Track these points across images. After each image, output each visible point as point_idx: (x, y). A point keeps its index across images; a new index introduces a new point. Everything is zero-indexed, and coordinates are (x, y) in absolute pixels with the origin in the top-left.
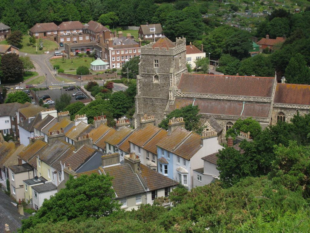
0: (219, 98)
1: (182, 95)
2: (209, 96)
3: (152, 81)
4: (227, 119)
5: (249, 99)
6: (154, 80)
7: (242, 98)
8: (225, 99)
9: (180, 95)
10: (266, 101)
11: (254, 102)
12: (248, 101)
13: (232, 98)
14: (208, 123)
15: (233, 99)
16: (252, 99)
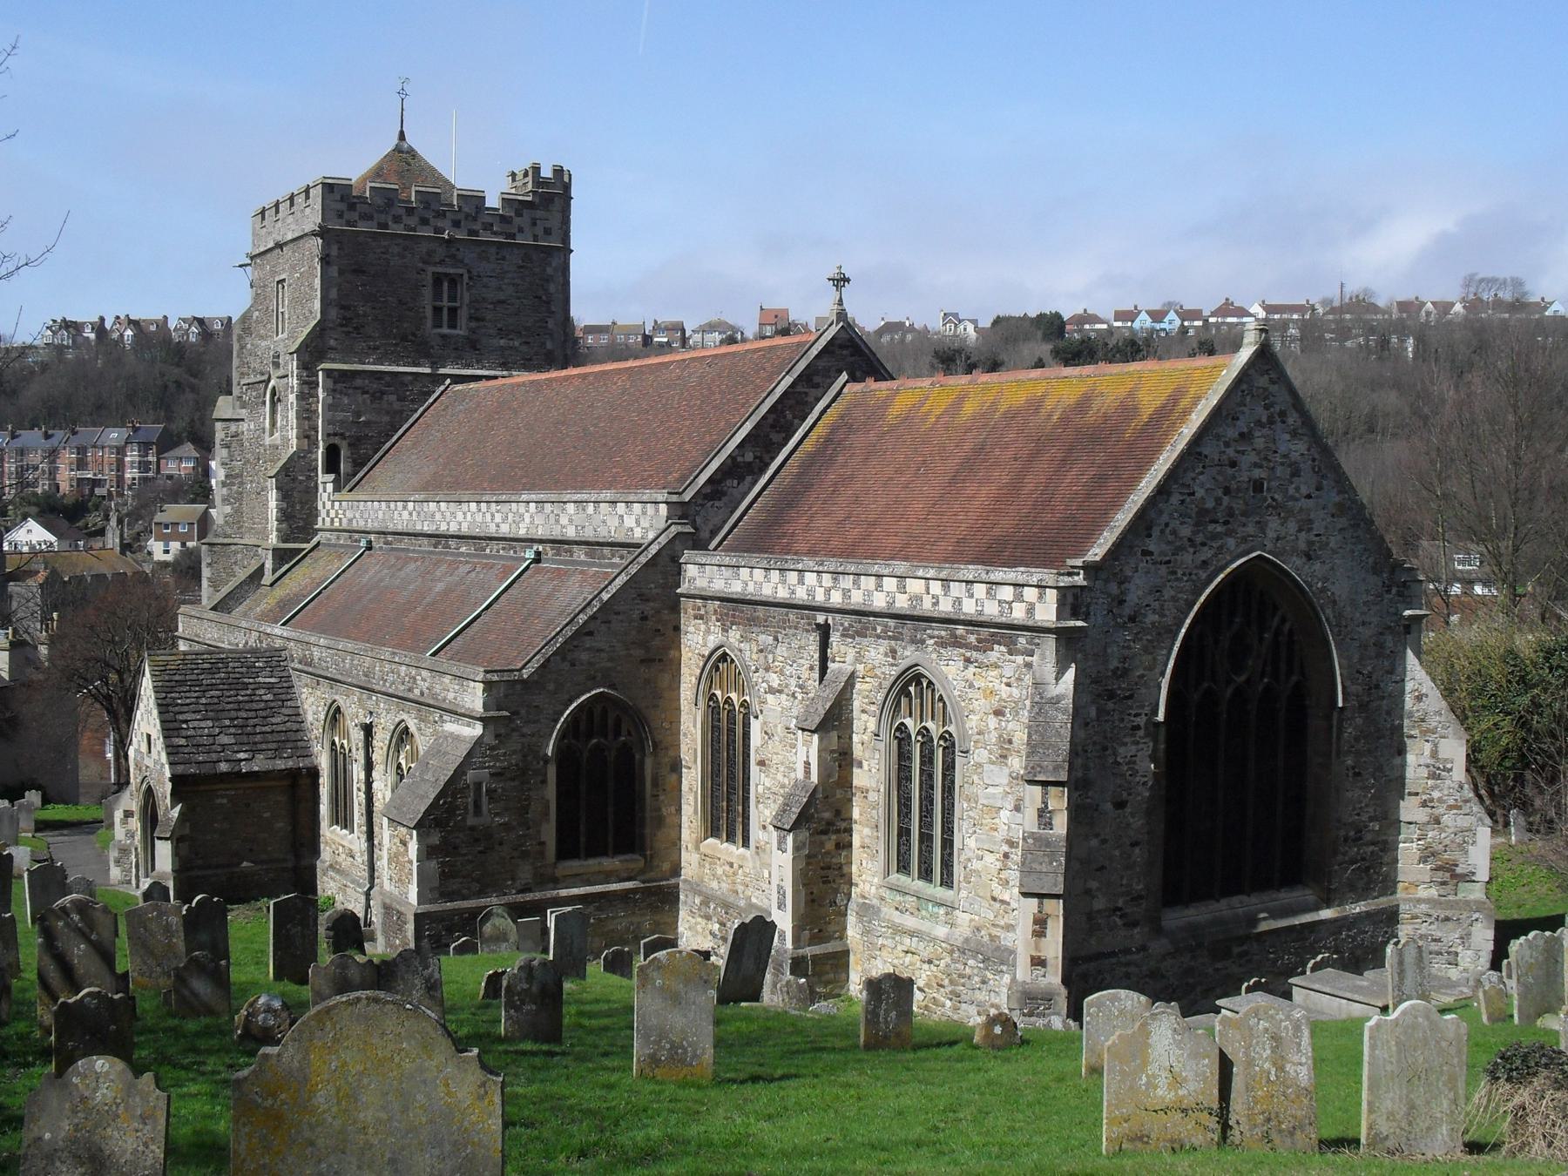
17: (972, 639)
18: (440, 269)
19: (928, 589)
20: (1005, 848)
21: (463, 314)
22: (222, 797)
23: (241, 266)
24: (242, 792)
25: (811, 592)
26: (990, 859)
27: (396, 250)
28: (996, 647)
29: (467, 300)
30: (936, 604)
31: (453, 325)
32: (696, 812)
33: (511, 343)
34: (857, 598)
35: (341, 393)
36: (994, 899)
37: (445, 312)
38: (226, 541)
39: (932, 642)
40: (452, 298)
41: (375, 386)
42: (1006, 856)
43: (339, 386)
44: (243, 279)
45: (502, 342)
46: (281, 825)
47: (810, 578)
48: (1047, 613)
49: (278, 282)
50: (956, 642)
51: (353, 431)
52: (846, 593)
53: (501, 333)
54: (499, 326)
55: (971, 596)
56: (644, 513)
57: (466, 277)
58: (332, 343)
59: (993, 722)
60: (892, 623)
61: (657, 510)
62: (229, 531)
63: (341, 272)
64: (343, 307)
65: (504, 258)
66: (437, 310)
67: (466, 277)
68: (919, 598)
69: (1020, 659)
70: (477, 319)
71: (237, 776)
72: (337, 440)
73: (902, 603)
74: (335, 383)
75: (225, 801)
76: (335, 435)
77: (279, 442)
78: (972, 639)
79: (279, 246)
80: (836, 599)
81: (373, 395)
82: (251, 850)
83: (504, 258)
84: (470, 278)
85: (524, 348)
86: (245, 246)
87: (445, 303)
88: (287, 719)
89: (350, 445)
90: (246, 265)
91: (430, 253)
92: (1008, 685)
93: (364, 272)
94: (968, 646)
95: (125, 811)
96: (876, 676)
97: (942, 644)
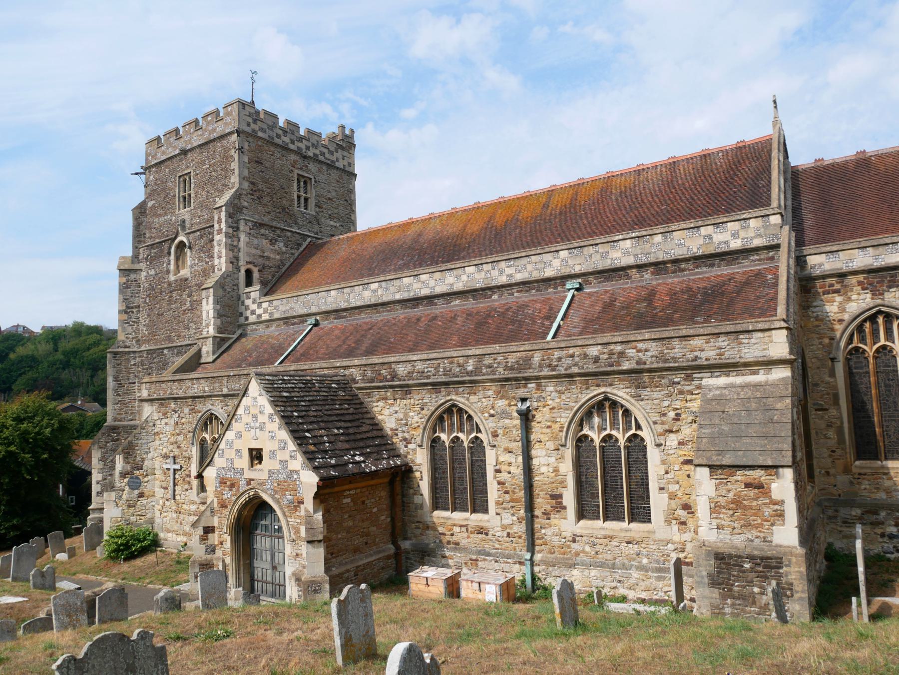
1: (266, 311)
2: (375, 291)
3: (168, 272)
4: (436, 386)
5: (605, 256)
6: (172, 267)
7: (556, 263)
8: (459, 286)
9: (258, 312)
10: (736, 244)
11: (640, 267)
12: (600, 267)
13: (495, 273)
15: (503, 280)
16: (626, 253)
18: (301, 173)
21: (312, 203)
22: (348, 496)
23: (136, 174)
24: (358, 491)
27: (279, 155)
29: (314, 195)
31: (306, 207)
32: (841, 441)
33: (335, 224)
35: (254, 236)
37: (302, 199)
38: (127, 350)
40: (306, 193)
41: (272, 235)
43: (252, 232)
44: (140, 181)
45: (332, 223)
46: (383, 518)
49: (180, 177)
51: (261, 261)
53: (331, 217)
54: (330, 213)
57: (313, 180)
58: (246, 204)
62: (128, 343)
63: (250, 161)
64: (252, 183)
65: (330, 174)
66: (299, 197)
67: (313, 180)
70: (320, 207)
71: (363, 475)
72: (250, 266)
74: (250, 229)
75: (349, 500)
76: (250, 263)
77: (189, 275)
79: (184, 152)
81: (271, 241)
82: (366, 543)
83: (330, 174)
84: (315, 182)
85: (341, 228)
86: (140, 162)
87: (302, 193)
88: (371, 428)
89: (259, 271)
90: (141, 173)
91: (295, 162)
93: (262, 164)
95: (205, 528)
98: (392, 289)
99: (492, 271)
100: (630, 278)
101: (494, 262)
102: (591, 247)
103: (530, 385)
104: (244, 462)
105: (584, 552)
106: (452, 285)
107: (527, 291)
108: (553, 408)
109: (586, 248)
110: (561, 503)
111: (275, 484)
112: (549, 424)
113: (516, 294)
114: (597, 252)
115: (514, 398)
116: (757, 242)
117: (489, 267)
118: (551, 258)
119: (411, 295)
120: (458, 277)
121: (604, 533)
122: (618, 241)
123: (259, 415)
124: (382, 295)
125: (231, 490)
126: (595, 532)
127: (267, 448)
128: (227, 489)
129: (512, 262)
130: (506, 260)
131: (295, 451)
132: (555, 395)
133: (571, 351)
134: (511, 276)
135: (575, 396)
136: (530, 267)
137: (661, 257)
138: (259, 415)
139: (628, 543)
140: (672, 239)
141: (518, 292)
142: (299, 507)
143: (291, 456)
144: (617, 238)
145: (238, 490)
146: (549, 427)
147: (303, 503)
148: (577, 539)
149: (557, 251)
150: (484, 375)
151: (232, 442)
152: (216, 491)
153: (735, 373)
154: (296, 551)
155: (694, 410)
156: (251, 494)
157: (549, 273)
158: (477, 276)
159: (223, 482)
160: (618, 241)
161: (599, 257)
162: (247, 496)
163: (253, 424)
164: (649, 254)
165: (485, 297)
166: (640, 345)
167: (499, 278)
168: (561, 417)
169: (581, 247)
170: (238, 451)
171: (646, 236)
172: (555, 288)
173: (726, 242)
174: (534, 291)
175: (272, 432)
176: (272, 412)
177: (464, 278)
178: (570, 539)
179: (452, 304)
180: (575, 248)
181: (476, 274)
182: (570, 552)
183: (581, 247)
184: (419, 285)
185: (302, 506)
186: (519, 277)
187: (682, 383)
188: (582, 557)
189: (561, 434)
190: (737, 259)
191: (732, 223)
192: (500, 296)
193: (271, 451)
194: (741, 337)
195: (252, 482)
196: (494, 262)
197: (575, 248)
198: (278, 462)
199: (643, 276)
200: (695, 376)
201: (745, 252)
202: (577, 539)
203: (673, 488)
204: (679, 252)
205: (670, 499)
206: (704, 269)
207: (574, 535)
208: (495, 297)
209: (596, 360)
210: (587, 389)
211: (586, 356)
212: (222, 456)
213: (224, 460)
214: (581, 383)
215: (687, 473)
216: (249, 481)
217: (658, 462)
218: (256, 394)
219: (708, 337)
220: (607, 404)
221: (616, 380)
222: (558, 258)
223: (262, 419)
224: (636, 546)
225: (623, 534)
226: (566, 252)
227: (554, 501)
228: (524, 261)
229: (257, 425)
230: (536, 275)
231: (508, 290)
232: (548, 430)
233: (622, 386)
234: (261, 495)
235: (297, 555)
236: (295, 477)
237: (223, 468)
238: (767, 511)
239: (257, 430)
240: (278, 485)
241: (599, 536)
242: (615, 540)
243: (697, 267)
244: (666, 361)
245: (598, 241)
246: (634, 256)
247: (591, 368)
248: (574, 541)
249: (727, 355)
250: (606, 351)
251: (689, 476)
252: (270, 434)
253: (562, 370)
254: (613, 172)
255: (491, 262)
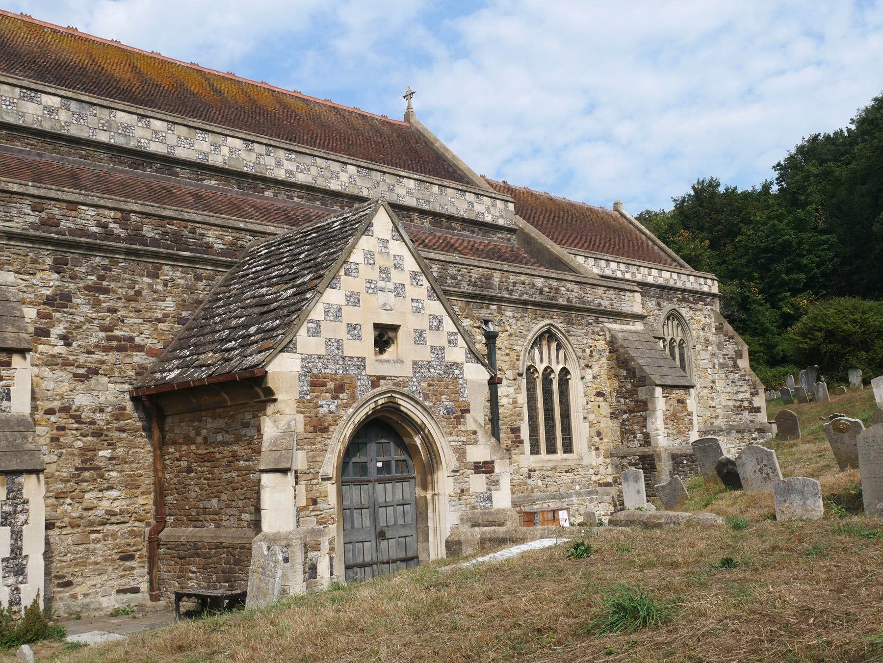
0: (156, 148)
2: (52, 111)
5: (391, 190)
8: (217, 160)
11: (423, 213)
13: (270, 161)
14: (398, 248)
15: (281, 174)
17: (691, 299)
19: (671, 276)
20: (712, 384)
25: (613, 272)
26: (705, 391)
28: (700, 303)
30: (675, 283)
34: (639, 277)
36: (710, 407)
39: (675, 300)
42: (712, 387)
47: (613, 265)
48: (715, 290)
50: (684, 300)
52: (633, 274)
55: (689, 281)
56: (494, 206)
59: (702, 333)
60: (658, 290)
61: (507, 206)
68: (668, 280)
69: (709, 307)
73: (661, 281)
78: (691, 299)
80: (628, 276)
92: (705, 317)
94: (690, 302)
96: (653, 315)
97: (680, 301)
98: (92, 121)
99: (266, 157)
100: (412, 221)
101: (271, 146)
102: (379, 173)
103: (492, 307)
104: (365, 347)
105: (538, 487)
106: (206, 155)
107: (310, 200)
108: (511, 335)
109: (374, 173)
110: (519, 437)
111: (424, 385)
112: (507, 351)
113: (296, 199)
114: (384, 181)
115: (478, 318)
116: (501, 222)
117: (262, 149)
118: (338, 170)
119: (133, 144)
120: (216, 147)
121: (551, 464)
122: (404, 177)
123: (392, 270)
124: (68, 124)
125: (335, 397)
126: (545, 465)
127: (409, 324)
128: (329, 395)
129: (293, 156)
130: (286, 149)
131: (456, 334)
132: (512, 321)
133: (523, 278)
134: (290, 173)
135: (527, 325)
136: (314, 171)
137: (438, 209)
138: (392, 270)
139: (567, 472)
140: (446, 194)
141: (299, 197)
142: (463, 417)
143: (449, 342)
144: (402, 174)
145: (353, 397)
146: (507, 355)
147: (468, 411)
148: (532, 474)
149: (346, 164)
150: (449, 286)
151: (340, 310)
152: (301, 400)
153: (619, 322)
154: (460, 486)
155: (600, 349)
156: (380, 402)
157: (334, 186)
158: (244, 155)
159: (317, 384)
160: (404, 177)
161: (386, 188)
162: (373, 406)
163: (381, 284)
164: (429, 202)
165: (255, 189)
166: (569, 285)
167: (276, 169)
168: (517, 345)
169: (370, 169)
170: (352, 327)
171: (427, 182)
172: (342, 207)
173: (483, 214)
174: (318, 203)
175: (417, 301)
176: (417, 269)
177: (225, 151)
178: (526, 475)
179: (205, 182)
180: (364, 167)
181: (242, 151)
182: (527, 489)
183: (370, 169)
184: (148, 134)
185: (467, 415)
186: (301, 178)
187: (594, 324)
188: (536, 494)
189: (518, 363)
190: (488, 232)
191: (487, 198)
192: (276, 195)
193: (416, 331)
194: (621, 293)
195: (382, 382)
196: (271, 146)
197: (364, 167)
198: (429, 349)
199: (423, 224)
200: (600, 319)
201: (494, 228)
202: (532, 474)
203: (591, 417)
204: (451, 210)
205: (590, 427)
206: (468, 233)
207: (530, 470)
208: (269, 193)
209: (541, 292)
210: (536, 319)
211: (534, 286)
212: (316, 332)
213: (321, 341)
214: (531, 312)
215: (598, 403)
216: (376, 381)
217: (583, 395)
218: (387, 235)
219: (606, 289)
220: (547, 335)
221: (555, 314)
222: (346, 172)
223: (397, 277)
224: (571, 474)
225: (563, 464)
226: (354, 168)
227: (513, 435)
228: (308, 160)
229: (391, 286)
230: (321, 183)
231: (287, 190)
232: (507, 358)
233: (559, 321)
234: (400, 402)
235: (462, 491)
236: (457, 372)
237: (319, 357)
238: (687, 421)
239: (392, 295)
240: (430, 385)
241: (548, 468)
242: (558, 470)
243: (463, 229)
244: (584, 303)
245: (385, 170)
246: (417, 199)
247: (538, 298)
248: (529, 477)
249: (614, 307)
250: (547, 284)
251: (599, 407)
252: (415, 304)
253: (516, 296)
254: (268, 84)
255: (267, 145)
